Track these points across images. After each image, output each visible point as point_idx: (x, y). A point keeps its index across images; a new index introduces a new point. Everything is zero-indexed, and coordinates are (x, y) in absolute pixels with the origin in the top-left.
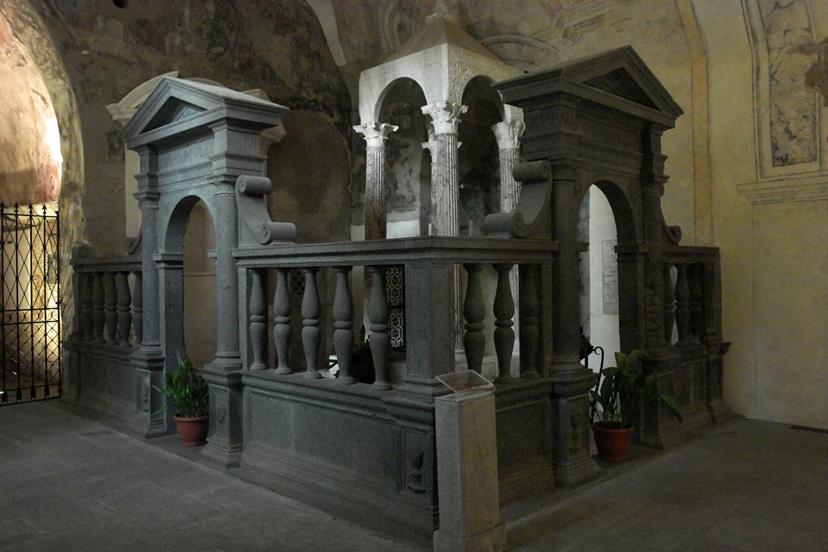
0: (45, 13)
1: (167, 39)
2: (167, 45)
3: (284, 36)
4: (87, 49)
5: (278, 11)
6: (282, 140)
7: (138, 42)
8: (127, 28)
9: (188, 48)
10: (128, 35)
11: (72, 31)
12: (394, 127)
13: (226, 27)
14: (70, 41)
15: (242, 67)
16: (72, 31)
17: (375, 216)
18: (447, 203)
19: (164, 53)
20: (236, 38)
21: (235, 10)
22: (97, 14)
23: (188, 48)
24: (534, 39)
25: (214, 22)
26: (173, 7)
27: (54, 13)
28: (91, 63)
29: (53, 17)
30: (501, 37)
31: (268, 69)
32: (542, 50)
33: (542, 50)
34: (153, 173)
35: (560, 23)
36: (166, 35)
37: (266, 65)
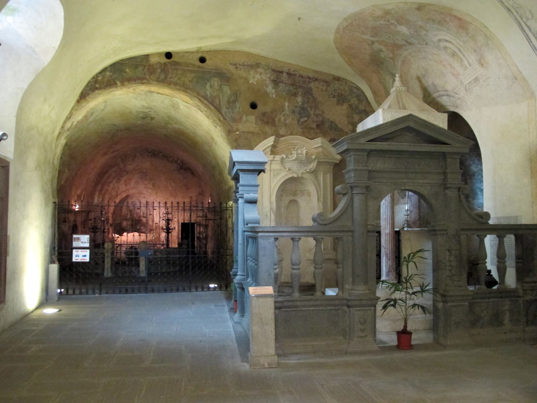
0: (221, 119)
1: (276, 119)
2: (277, 122)
3: (342, 105)
4: (239, 131)
5: (339, 93)
6: (340, 161)
7: (262, 124)
9: (287, 121)
11: (232, 124)
13: (308, 107)
15: (318, 126)
16: (232, 124)
19: (275, 126)
21: (313, 97)
23: (287, 121)
27: (224, 118)
28: (240, 137)
29: (224, 120)
31: (333, 124)
32: (459, 99)
33: (459, 99)
34: (237, 191)
35: (462, 83)
36: (276, 117)
37: (332, 122)
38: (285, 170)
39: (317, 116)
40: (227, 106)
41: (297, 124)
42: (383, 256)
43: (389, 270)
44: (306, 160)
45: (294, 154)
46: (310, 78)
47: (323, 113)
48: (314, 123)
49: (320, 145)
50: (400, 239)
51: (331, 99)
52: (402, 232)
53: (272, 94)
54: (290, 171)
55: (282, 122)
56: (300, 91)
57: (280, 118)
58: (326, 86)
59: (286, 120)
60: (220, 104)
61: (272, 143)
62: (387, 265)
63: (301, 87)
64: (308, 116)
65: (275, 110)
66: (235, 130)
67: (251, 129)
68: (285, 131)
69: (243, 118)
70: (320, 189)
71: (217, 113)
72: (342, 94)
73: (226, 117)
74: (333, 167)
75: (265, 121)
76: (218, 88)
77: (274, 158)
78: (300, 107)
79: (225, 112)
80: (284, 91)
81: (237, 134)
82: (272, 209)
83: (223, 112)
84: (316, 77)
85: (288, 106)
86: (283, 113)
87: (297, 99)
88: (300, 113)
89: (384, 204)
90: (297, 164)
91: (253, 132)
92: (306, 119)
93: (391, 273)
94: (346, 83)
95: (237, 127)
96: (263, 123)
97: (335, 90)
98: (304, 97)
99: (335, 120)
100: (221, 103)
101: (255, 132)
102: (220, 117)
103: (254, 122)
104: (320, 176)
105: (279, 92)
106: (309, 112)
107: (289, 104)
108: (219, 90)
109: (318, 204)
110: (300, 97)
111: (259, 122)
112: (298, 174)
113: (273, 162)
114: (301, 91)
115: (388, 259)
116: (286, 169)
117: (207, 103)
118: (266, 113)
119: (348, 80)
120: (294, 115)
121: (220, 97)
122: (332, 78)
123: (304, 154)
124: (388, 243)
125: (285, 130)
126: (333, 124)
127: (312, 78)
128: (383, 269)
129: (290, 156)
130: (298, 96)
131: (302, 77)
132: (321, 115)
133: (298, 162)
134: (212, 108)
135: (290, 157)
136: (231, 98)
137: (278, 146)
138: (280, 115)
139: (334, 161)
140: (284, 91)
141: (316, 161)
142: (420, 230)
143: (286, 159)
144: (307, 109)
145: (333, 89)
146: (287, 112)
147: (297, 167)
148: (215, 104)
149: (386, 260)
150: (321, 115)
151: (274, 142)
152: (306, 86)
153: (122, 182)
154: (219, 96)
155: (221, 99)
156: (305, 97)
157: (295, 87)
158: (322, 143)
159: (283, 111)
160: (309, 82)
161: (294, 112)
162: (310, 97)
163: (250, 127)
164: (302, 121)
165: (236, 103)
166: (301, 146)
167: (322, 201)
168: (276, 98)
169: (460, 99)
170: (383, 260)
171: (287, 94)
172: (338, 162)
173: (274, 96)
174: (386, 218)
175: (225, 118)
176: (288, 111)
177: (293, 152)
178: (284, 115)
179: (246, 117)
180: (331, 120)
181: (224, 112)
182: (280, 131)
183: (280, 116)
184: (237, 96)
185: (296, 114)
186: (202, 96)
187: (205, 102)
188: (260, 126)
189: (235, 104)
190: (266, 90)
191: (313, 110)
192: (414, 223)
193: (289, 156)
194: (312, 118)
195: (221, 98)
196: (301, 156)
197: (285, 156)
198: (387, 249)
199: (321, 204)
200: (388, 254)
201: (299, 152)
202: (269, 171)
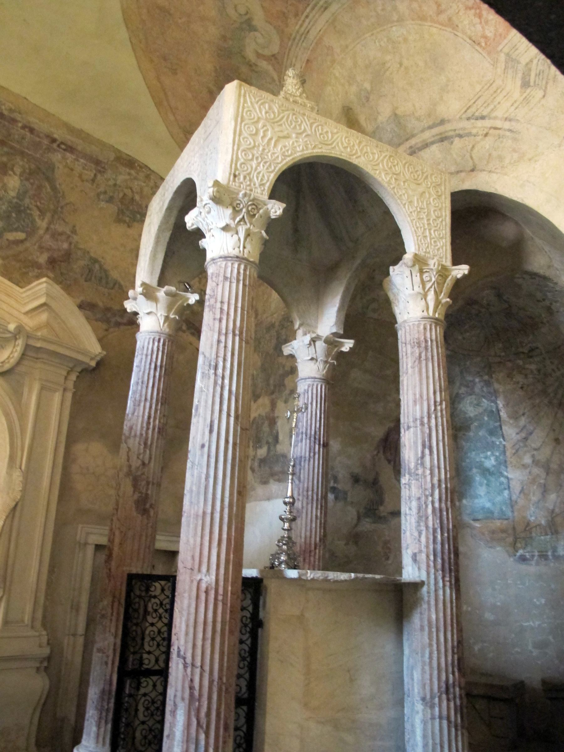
3: (129, 226)
5: (125, 195)
12: (189, 295)
13: (35, 208)
15: (52, 262)
17: (130, 466)
18: (205, 419)
20: (50, 223)
21: (54, 188)
24: (468, 119)
25: (15, 200)
30: (413, 142)
33: (486, 135)
37: (95, 261)
39: (55, 235)
42: (174, 713)
46: (54, 140)
47: (74, 232)
48: (42, 253)
49: (42, 300)
50: (261, 615)
51: (103, 204)
52: (272, 586)
56: (19, 164)
58: (94, 171)
63: (22, 154)
64: (31, 231)
72: (133, 199)
74: (78, 377)
78: (10, 202)
84: (69, 143)
87: (5, 181)
89: (203, 446)
92: (21, 236)
94: (148, 177)
97: (115, 185)
98: (27, 179)
99: (103, 258)
104: (30, 391)
106: (33, 221)
110: (16, 178)
114: (21, 163)
119: (153, 171)
122: (112, 156)
124: (204, 639)
126: (97, 266)
127: (58, 143)
130: (11, 172)
131: (32, 130)
132: (69, 237)
139: (80, 357)
141: (20, 342)
142: (356, 578)
144: (28, 211)
145: (111, 183)
150: (69, 237)
152: (38, 156)
156: (32, 181)
157: (5, 149)
158: (48, 295)
160: (49, 149)
164: (7, 240)
167: (23, 467)
169: (492, 131)
170: (173, 725)
172: (93, 364)
174: (204, 513)
180: (92, 255)
191: (46, 220)
192: (307, 552)
194: (41, 238)
198: (198, 671)
199: (17, 476)
200: (199, 700)
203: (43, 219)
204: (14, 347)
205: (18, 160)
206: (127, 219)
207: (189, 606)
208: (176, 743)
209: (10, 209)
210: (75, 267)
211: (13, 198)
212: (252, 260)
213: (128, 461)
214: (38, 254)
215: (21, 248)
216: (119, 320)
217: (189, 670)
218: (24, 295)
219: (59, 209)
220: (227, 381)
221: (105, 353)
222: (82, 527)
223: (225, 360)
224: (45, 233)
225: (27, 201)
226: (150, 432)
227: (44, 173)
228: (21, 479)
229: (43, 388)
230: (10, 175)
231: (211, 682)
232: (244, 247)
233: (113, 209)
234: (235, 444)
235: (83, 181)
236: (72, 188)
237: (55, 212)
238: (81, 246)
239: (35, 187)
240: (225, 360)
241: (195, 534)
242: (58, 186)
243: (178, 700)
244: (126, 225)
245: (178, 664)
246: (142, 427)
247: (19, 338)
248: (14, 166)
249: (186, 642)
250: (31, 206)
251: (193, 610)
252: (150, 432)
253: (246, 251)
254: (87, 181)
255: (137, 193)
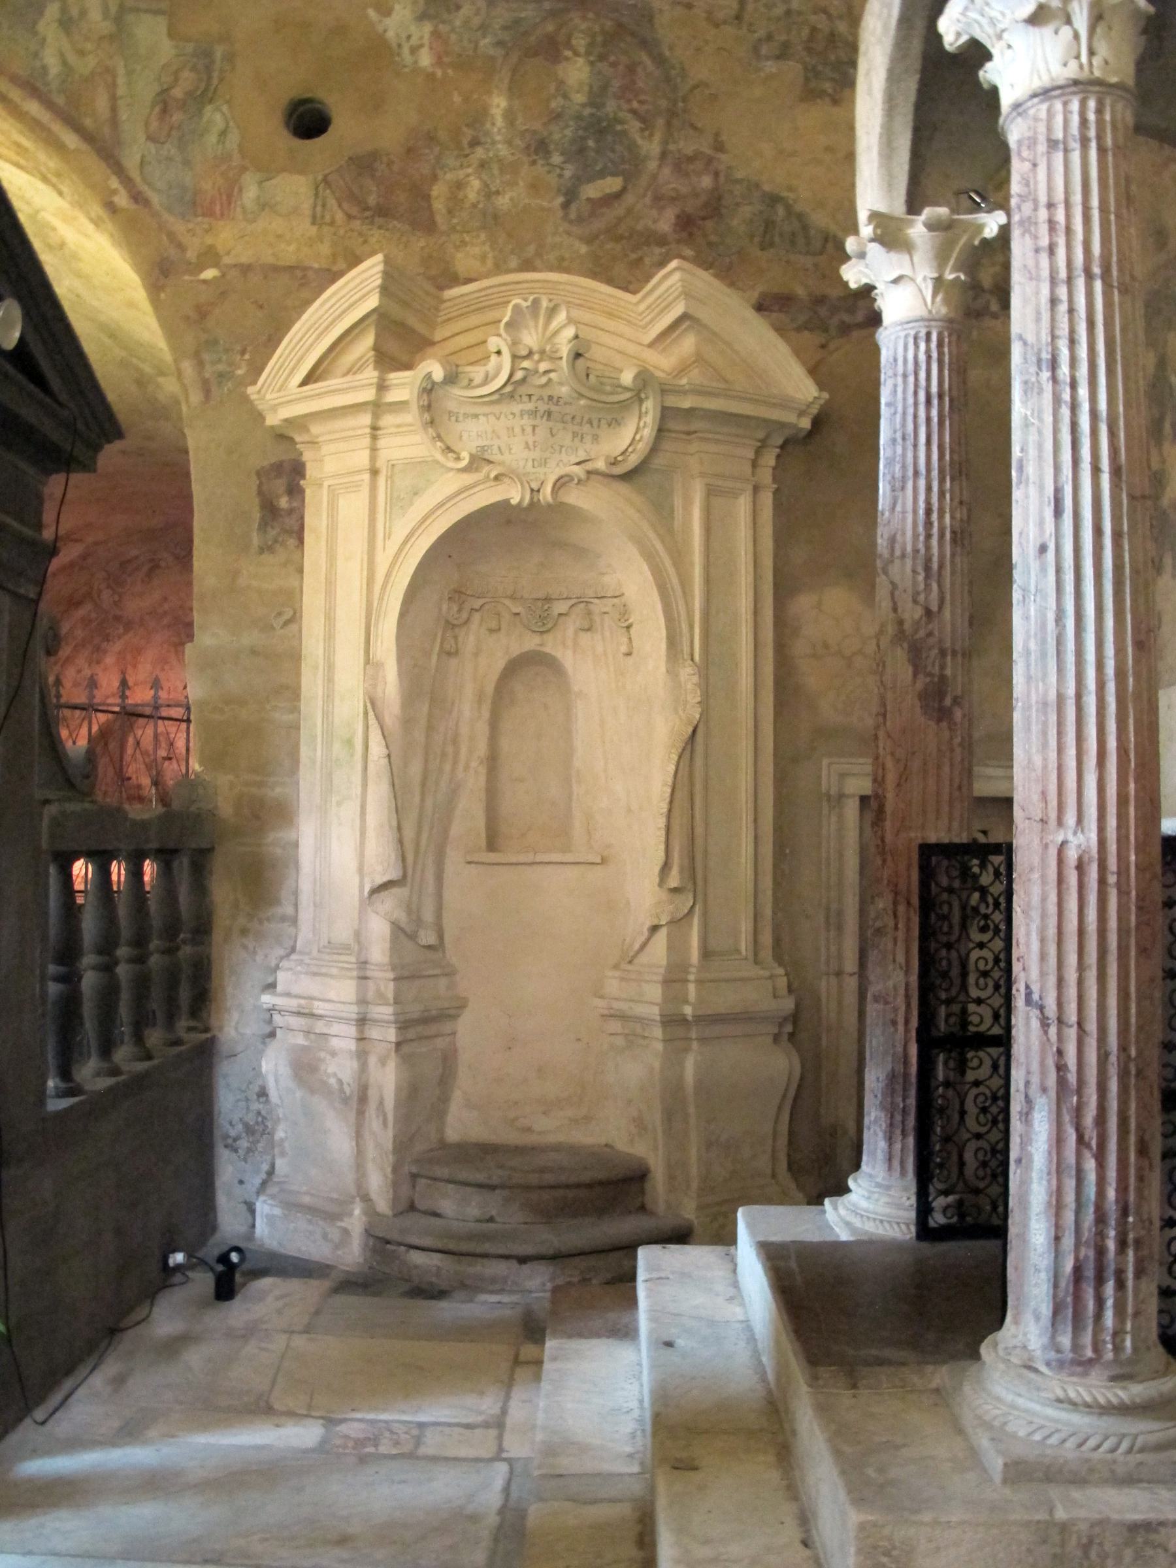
0: (116, 199)
1: (439, 191)
2: (439, 205)
4: (216, 265)
5: (814, 29)
6: (817, 422)
7: (350, 217)
8: (321, 188)
9: (503, 202)
10: (324, 206)
11: (179, 227)
12: (982, 217)
13: (629, 116)
14: (172, 252)
15: (686, 223)
16: (179, 227)
17: (901, 622)
18: (1041, 488)
19: (429, 226)
20: (665, 142)
21: (660, 61)
22: (244, 169)
23: (503, 202)
25: (587, 111)
26: (457, 98)
27: (137, 197)
28: (223, 294)
29: (133, 207)
31: (781, 211)
36: (435, 178)
37: (773, 200)
38: (451, 464)
39: (682, 165)
40: (154, 124)
41: (560, 213)
42: (1027, 1116)
43: (1089, 1253)
44: (582, 396)
45: (499, 353)
47: (719, 147)
48: (661, 209)
49: (678, 310)
51: (770, 67)
53: (414, 50)
54: (486, 468)
55: (474, 206)
57: (460, 185)
59: (498, 193)
60: (114, 121)
61: (373, 302)
62: (1070, 1198)
64: (630, 167)
65: (431, 138)
66: (194, 260)
67: (289, 253)
68: (490, 255)
69: (241, 190)
70: (685, 583)
71: (98, 168)
73: (144, 188)
74: (778, 457)
75: (372, 200)
76: (107, 27)
77: (382, 387)
78: (579, 118)
79: (142, 163)
80: (484, 28)
81: (205, 282)
82: (373, 703)
83: (131, 161)
85: (509, 116)
86: (480, 153)
87: (561, 74)
88: (578, 152)
89: (1043, 549)
90: (527, 422)
91: (297, 267)
92: (613, 184)
93: (1110, 1288)
95: (209, 240)
96: (354, 211)
97: (788, 13)
98: (602, 58)
100: (124, 115)
101: (311, 268)
102: (115, 192)
103: (306, 207)
105: (453, 37)
106: (632, 147)
107: (510, 98)
108: (111, 38)
109: (672, 672)
110: (581, 61)
111: (335, 207)
112: (535, 486)
113: (388, 420)
114: (584, 26)
115: (1081, 1140)
116: (458, 459)
117: (45, 116)
118: (374, 155)
120: (541, 162)
121: (114, 77)
123: (565, 350)
124: (1081, 967)
125: (487, 248)
126: (781, 211)
128: (1023, 1238)
129: (478, 373)
130: (568, 53)
132: (710, 160)
133: (529, 406)
134: (71, 140)
135: (478, 379)
136: (176, 80)
137: (438, 335)
138: (462, 166)
139: (776, 415)
140: (484, 28)
141: (650, 406)
143: (456, 391)
144: (619, 128)
145: (779, 10)
146: (503, 150)
147: (530, 439)
148: (88, 122)
149: (1059, 1141)
150: (710, 160)
151: (384, 290)
153: (109, 660)
154: (110, 71)
155: (121, 91)
156: (612, 58)
158: (687, 294)
159: (475, 143)
161: (541, 147)
162: (645, 58)
163: (279, 237)
164: (588, 199)
165: (208, 109)
166: (536, 302)
167: (697, 657)
168: (439, 73)
170: (1026, 1141)
171: (500, 43)
172: (806, 423)
173: (425, 59)
174: (1061, 699)
175: (140, 193)
176: (509, 143)
177: (494, 343)
178: (483, 165)
179: (260, 183)
180: (767, 188)
181: (138, 157)
182: (459, 255)
183: (461, 174)
184: (209, 69)
185: (557, 159)
186: (14, 79)
187: (33, 108)
188: (342, 232)
189: (200, 112)
190: (380, 29)
191: (658, 137)
193: (469, 369)
194: (654, 177)
195: (121, 81)
196: (543, 367)
197: (438, 374)
198: (1072, 1033)
199: (688, 675)
200: (1080, 1091)
201: (530, 339)
202: (366, 476)
203: (651, 135)
204: (640, 418)
205: (577, 21)
206: (828, 86)
207: (1044, 899)
208: (1035, 1175)
209: (580, 133)
210: (735, 223)
211: (584, 105)
212: (1114, 80)
213: (895, 610)
214: (654, 212)
215: (619, 210)
216: (846, 318)
217: (1053, 1030)
218: (642, 307)
219: (680, 104)
220: (1083, 392)
221: (826, 395)
222: (830, 765)
223: (1072, 342)
224: (660, 166)
225: (611, 106)
226: (934, 542)
227: (633, 34)
228: (695, 679)
229: (711, 492)
230: (567, 59)
231: (1103, 1058)
232: (1092, 53)
233: (792, 69)
234: (1117, 535)
235: (717, 26)
236: (698, 49)
237: (672, 114)
238: (739, 175)
239: (621, 68)
240: (1072, 342)
241: (1045, 745)
242: (667, 53)
243: (1034, 1090)
244: (827, 99)
245: (1028, 1019)
246: (915, 536)
247: (647, 398)
248: (569, 37)
249: (1043, 974)
250: (621, 114)
251: (1052, 909)
252: (934, 542)
253: (1096, 61)
254: (725, 22)
255: (840, 17)
